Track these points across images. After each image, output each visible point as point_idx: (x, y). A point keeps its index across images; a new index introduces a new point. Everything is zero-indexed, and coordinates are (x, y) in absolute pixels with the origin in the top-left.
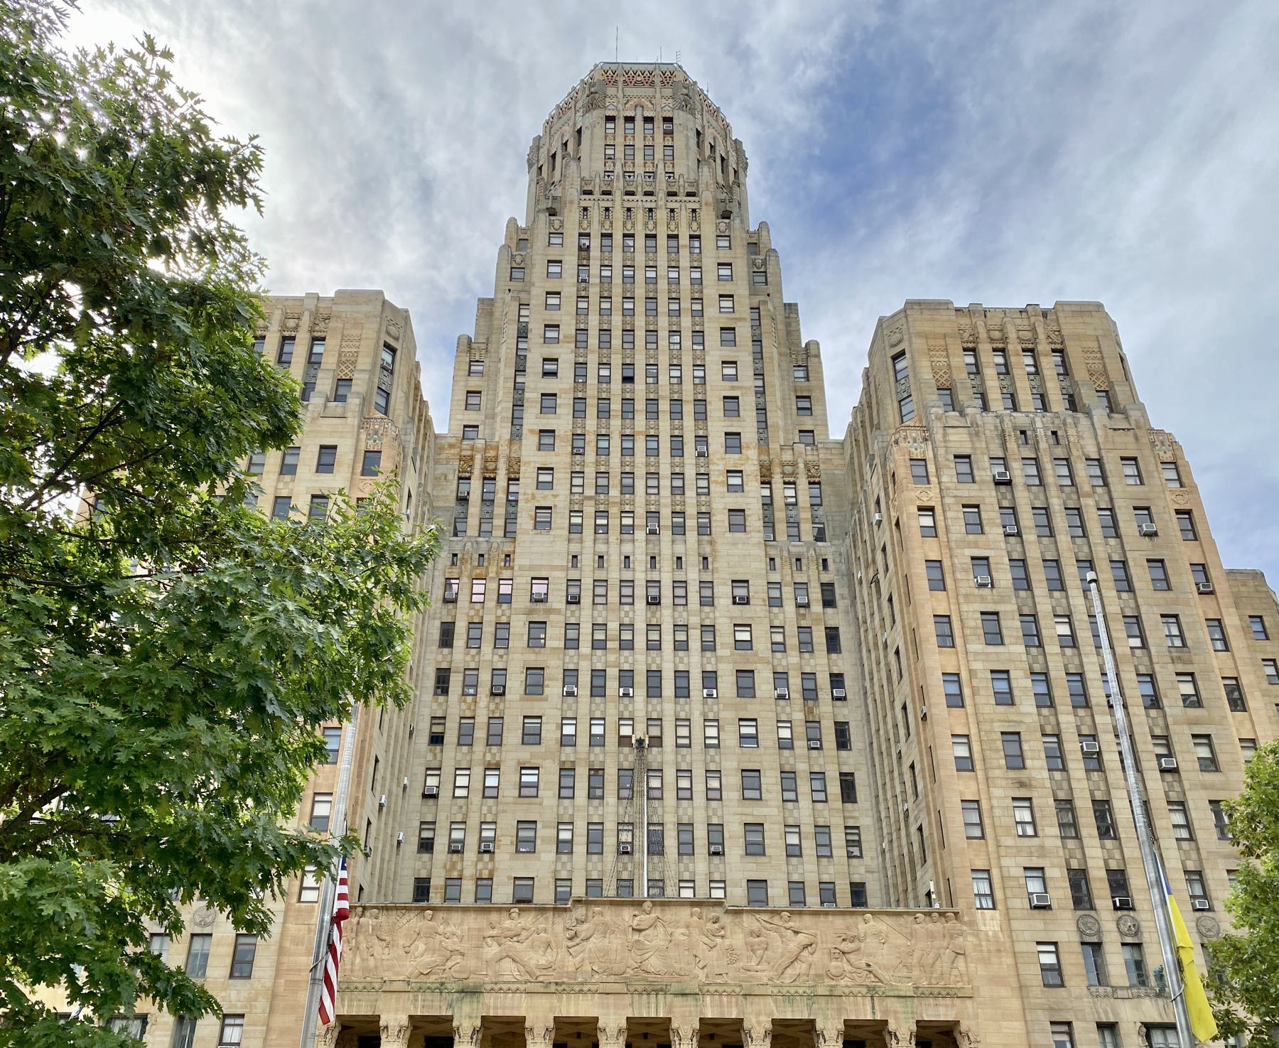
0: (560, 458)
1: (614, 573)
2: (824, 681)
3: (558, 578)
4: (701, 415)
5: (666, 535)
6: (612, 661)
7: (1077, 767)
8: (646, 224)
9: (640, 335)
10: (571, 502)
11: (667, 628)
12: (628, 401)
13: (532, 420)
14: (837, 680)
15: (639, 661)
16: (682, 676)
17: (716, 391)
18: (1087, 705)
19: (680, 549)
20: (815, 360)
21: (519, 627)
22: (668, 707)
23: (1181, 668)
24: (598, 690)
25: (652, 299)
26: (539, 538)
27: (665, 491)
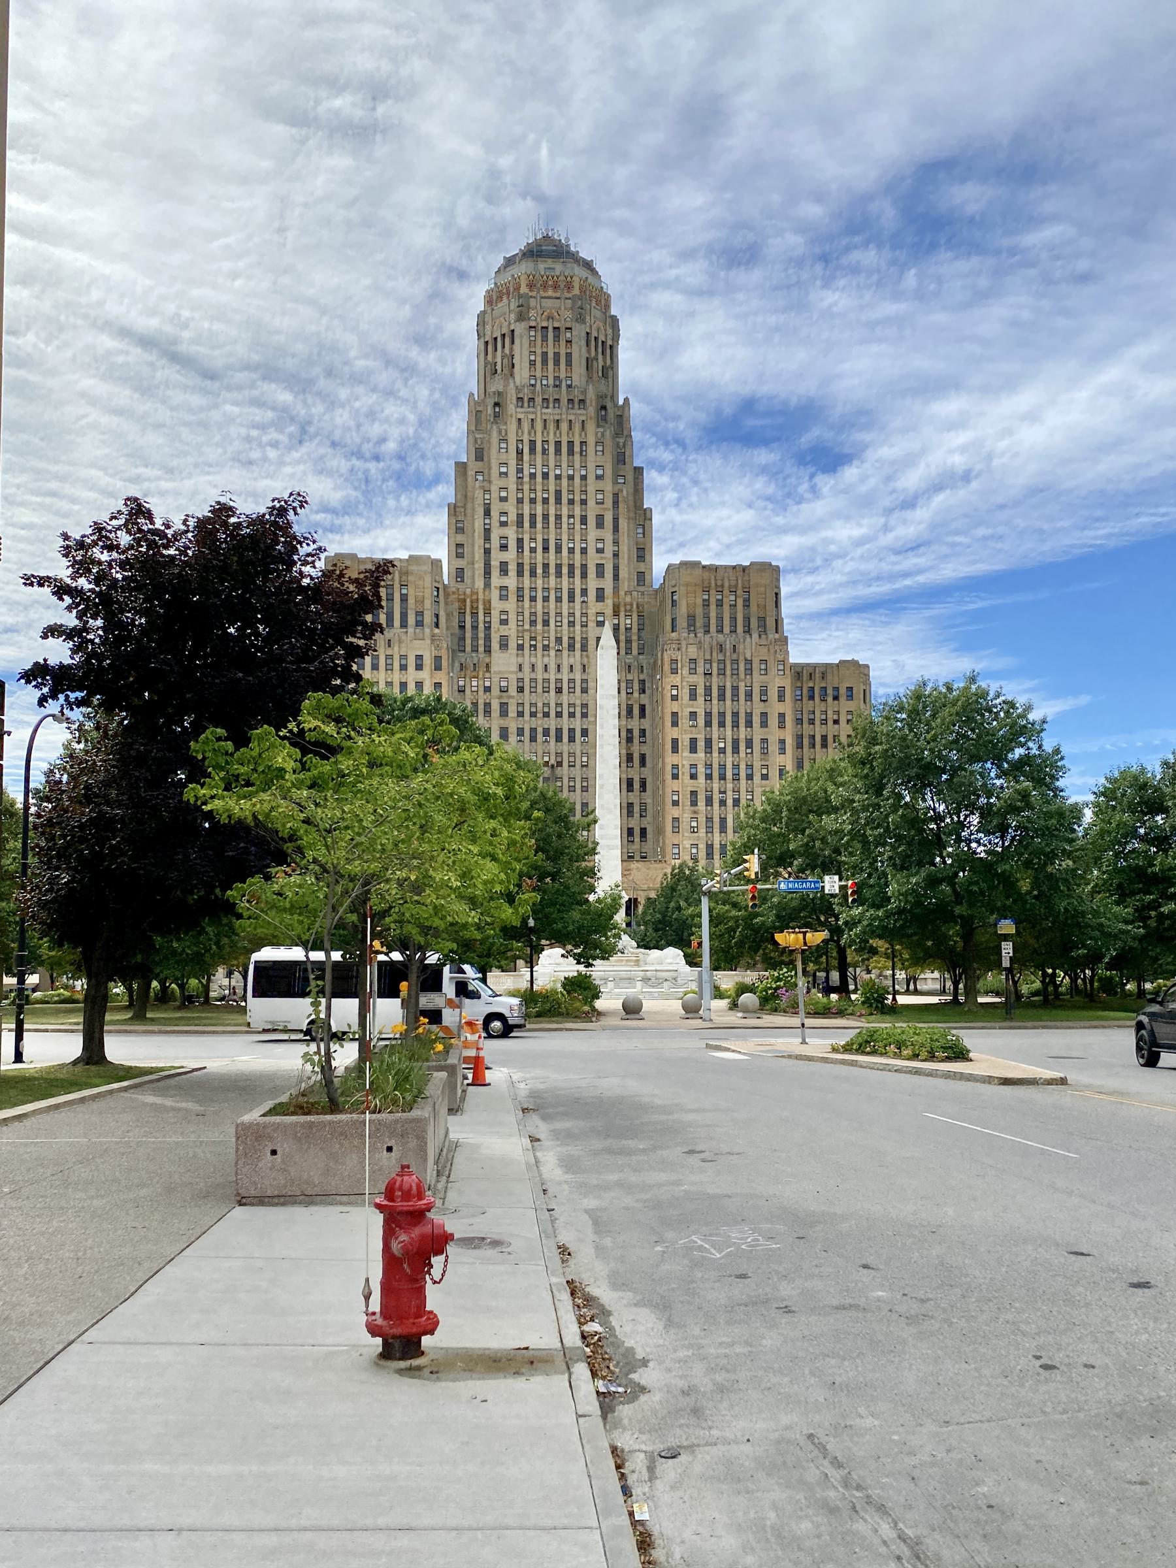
0: (511, 605)
1: (540, 675)
2: (636, 733)
3: (513, 678)
4: (584, 575)
5: (565, 653)
6: (540, 723)
7: (716, 805)
8: (555, 434)
9: (552, 519)
10: (518, 631)
11: (565, 706)
12: (546, 566)
13: (496, 580)
14: (643, 732)
15: (552, 723)
16: (572, 731)
17: (593, 559)
18: (725, 779)
19: (572, 661)
20: (648, 522)
21: (495, 706)
22: (565, 746)
23: (764, 763)
24: (533, 739)
25: (558, 494)
26: (502, 655)
27: (565, 626)
